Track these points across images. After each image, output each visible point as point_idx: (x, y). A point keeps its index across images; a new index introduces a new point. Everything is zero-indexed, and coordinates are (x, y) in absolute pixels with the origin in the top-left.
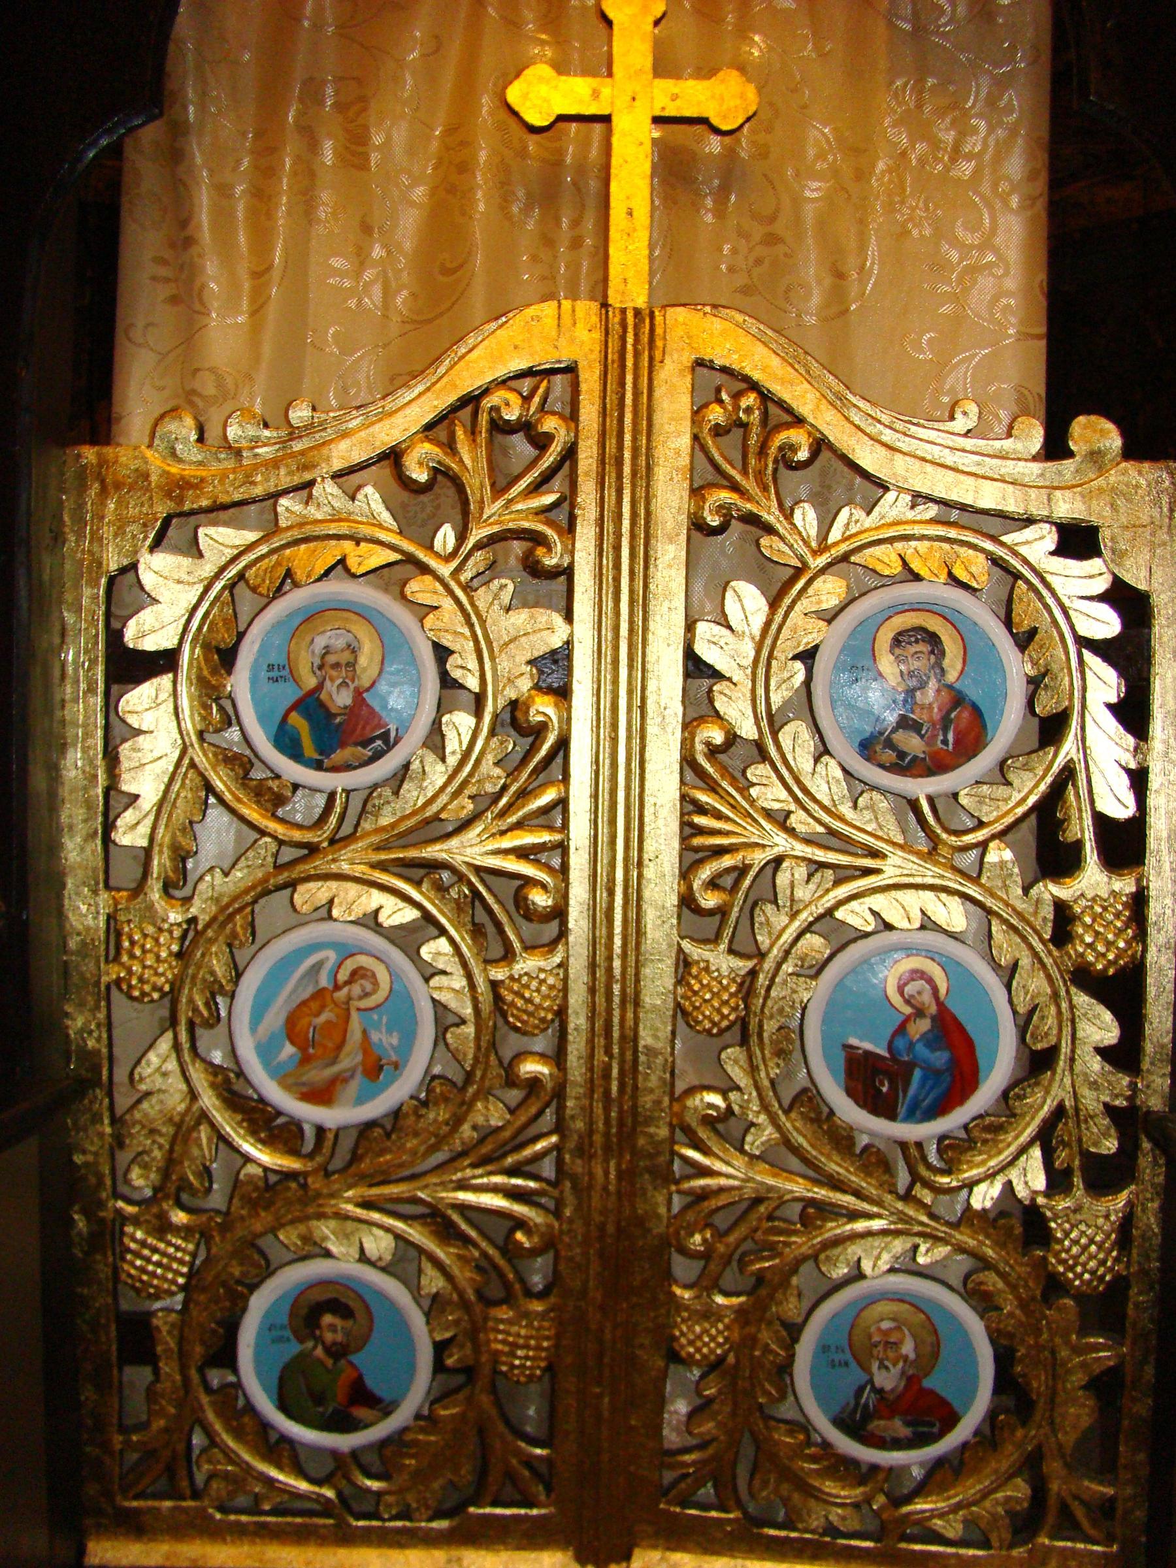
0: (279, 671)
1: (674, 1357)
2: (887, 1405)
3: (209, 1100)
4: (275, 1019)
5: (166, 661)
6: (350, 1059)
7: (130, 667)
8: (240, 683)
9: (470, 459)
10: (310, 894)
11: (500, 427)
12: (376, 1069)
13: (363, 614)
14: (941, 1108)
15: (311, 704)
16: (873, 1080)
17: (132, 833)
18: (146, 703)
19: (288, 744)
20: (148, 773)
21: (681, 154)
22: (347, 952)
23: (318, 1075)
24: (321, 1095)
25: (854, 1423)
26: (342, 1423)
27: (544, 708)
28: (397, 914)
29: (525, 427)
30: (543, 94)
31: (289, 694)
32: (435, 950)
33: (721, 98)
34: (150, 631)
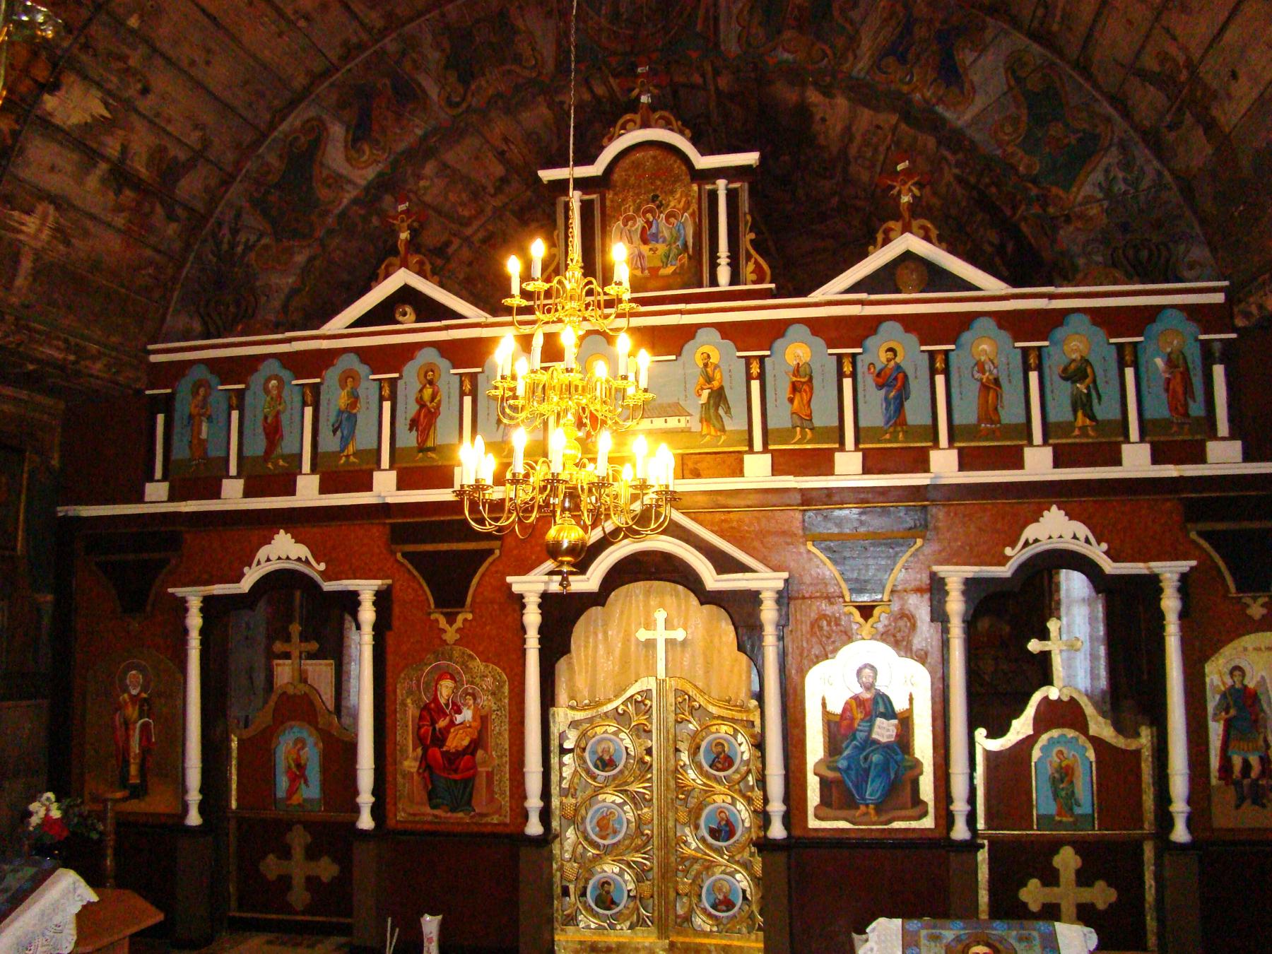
0: (593, 752)
1: (678, 894)
2: (721, 902)
3: (581, 840)
4: (595, 821)
5: (571, 751)
6: (610, 831)
7: (563, 752)
8: (587, 755)
9: (631, 708)
10: (600, 797)
11: (636, 701)
12: (615, 832)
13: (610, 740)
14: (728, 839)
15: (601, 759)
16: (714, 833)
17: (565, 785)
18: (567, 759)
19: (596, 766)
20: (567, 772)
21: (670, 643)
22: (609, 808)
23: (604, 833)
24: (603, 838)
25: (714, 907)
26: (609, 909)
27: (647, 758)
28: (619, 801)
29: (642, 702)
30: (643, 635)
31: (596, 757)
32: (627, 808)
33: (679, 635)
34: (568, 745)
